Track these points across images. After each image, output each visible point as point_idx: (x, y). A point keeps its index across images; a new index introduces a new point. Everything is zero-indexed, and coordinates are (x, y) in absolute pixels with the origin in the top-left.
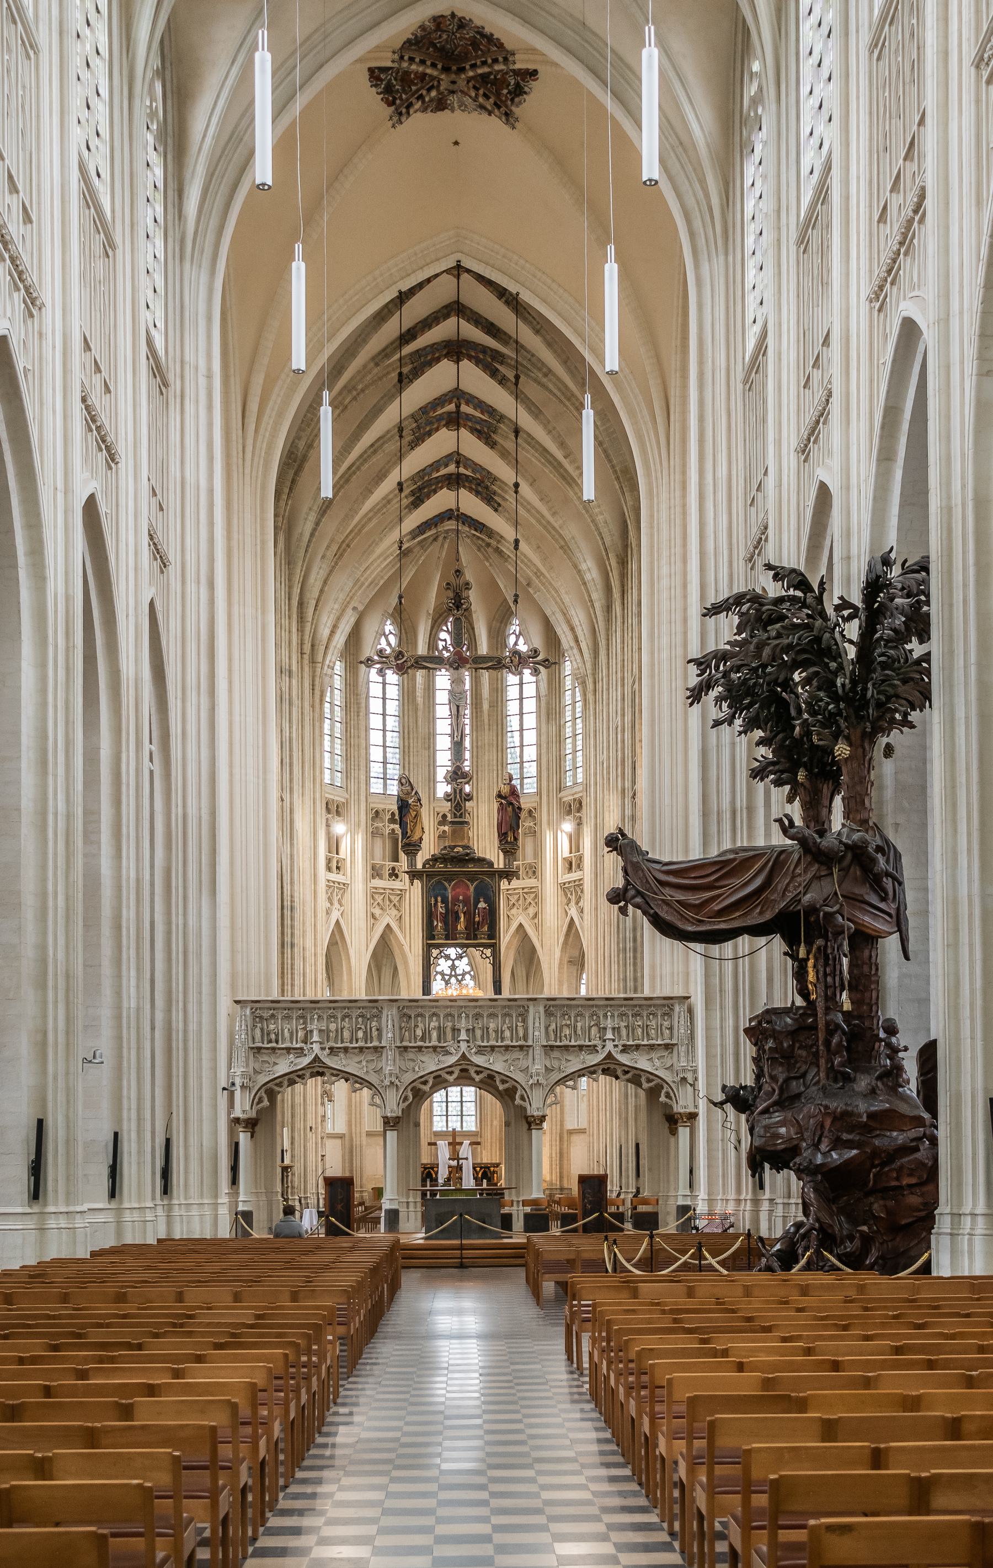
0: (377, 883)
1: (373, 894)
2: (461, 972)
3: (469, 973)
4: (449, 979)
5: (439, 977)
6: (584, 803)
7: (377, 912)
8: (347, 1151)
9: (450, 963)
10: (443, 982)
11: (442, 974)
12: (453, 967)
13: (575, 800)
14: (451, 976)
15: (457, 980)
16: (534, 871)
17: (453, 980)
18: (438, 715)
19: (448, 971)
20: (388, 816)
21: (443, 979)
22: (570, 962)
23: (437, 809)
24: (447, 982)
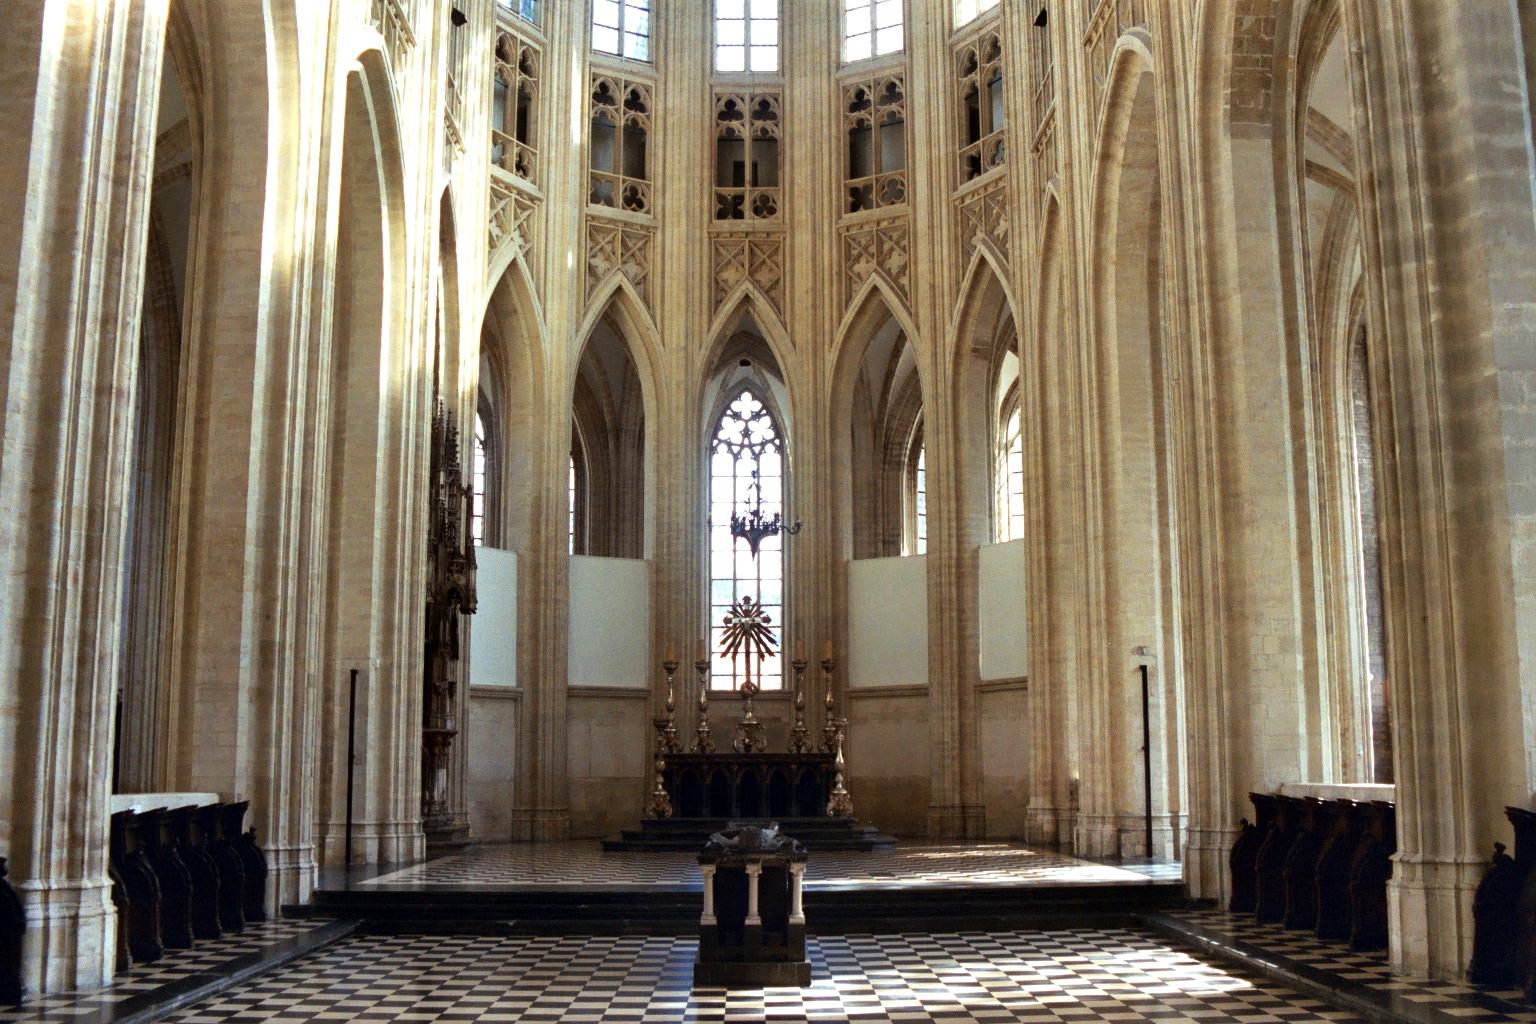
0: (601, 210)
1: (593, 230)
2: (759, 441)
3: (772, 441)
4: (739, 452)
5: (723, 448)
6: (1001, 43)
7: (600, 263)
8: (527, 725)
9: (741, 425)
10: (731, 457)
11: (729, 444)
12: (746, 433)
13: (981, 40)
14: (742, 446)
15: (753, 453)
16: (896, 192)
17: (746, 452)
18: (721, 38)
19: (737, 439)
20: (621, 97)
21: (730, 451)
22: (975, 350)
23: (717, 90)
24: (736, 457)
